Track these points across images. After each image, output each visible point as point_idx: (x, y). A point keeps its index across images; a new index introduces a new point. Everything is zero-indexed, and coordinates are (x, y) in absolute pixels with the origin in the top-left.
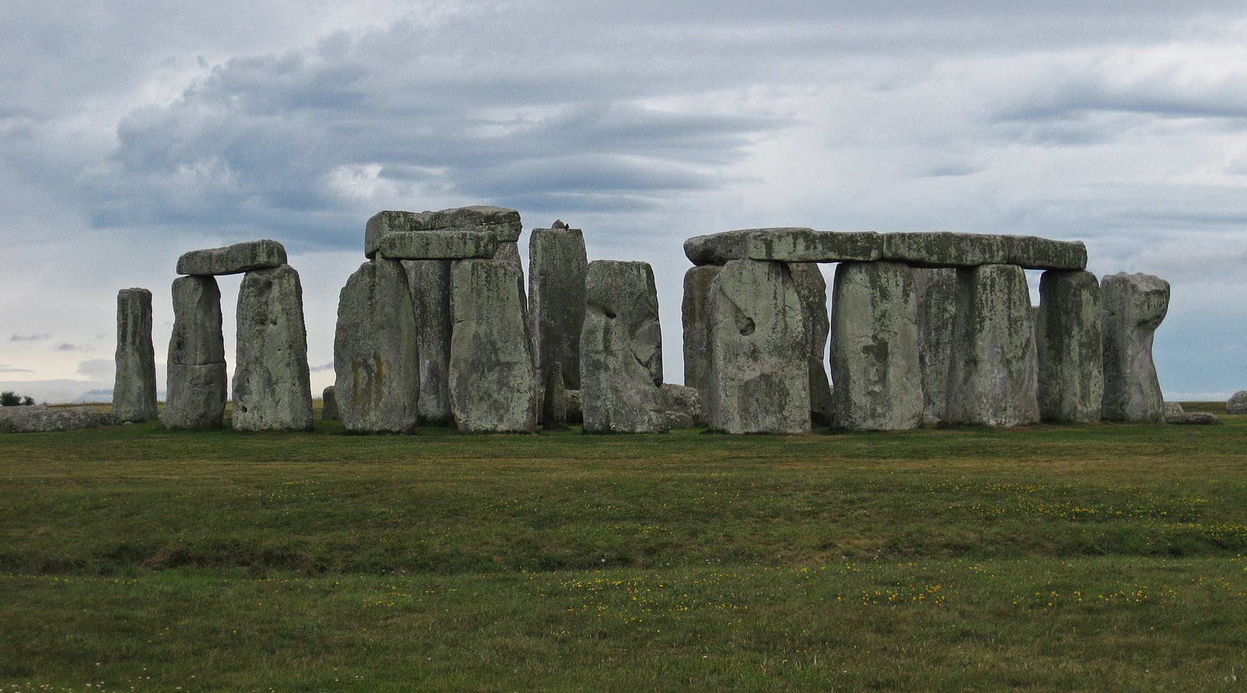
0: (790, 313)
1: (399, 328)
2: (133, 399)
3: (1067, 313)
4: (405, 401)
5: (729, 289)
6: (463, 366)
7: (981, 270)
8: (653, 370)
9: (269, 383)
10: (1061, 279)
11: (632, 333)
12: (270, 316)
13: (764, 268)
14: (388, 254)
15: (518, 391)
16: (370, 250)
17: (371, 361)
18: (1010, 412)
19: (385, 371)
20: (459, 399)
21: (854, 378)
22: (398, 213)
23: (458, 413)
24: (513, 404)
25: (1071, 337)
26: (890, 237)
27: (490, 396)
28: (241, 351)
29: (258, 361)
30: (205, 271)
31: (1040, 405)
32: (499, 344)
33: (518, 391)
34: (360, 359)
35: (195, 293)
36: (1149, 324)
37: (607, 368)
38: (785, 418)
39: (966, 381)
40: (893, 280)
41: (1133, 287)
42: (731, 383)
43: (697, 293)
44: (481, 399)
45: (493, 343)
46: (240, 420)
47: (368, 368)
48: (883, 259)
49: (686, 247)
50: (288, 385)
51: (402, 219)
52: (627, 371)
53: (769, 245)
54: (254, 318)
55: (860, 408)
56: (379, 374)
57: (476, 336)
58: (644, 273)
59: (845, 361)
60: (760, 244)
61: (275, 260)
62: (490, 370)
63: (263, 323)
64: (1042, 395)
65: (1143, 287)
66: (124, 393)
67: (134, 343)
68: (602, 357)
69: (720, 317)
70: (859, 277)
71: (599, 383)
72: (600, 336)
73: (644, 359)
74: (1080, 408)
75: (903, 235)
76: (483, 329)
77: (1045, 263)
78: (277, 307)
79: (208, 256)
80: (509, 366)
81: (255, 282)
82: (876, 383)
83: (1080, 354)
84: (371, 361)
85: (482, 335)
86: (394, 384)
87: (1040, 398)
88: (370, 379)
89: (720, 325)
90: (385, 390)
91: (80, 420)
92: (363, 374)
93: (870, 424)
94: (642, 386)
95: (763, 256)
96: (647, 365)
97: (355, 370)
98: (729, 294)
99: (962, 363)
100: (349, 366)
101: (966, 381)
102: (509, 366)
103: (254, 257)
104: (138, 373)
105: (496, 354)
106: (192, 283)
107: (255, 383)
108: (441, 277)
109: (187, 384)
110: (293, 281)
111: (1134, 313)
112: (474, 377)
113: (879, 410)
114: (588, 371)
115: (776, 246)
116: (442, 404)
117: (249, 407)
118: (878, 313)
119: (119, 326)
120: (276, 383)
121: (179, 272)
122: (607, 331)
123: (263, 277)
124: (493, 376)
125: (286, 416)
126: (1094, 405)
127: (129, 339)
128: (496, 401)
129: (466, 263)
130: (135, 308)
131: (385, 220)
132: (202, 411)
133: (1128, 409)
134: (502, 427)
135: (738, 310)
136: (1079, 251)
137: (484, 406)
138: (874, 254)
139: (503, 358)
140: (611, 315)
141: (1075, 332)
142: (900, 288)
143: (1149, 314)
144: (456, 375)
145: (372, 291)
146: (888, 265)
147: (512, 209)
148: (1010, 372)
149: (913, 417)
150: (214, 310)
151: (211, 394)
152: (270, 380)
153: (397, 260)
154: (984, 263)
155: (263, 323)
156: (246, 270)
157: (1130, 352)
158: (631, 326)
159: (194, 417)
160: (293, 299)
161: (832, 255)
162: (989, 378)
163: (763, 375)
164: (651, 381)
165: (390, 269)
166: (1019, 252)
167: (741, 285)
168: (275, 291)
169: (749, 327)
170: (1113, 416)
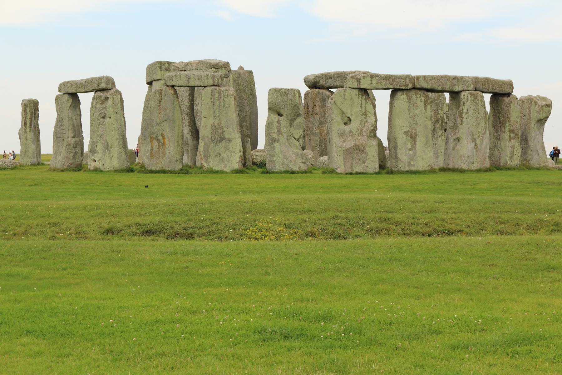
0: (369, 114)
1: (174, 121)
2: (30, 155)
3: (503, 115)
4: (177, 157)
5: (338, 103)
6: (206, 140)
7: (462, 94)
8: (301, 143)
9: (107, 147)
10: (500, 98)
11: (291, 124)
12: (108, 114)
13: (356, 92)
14: (168, 84)
15: (234, 152)
16: (149, 80)
17: (160, 137)
18: (476, 164)
19: (167, 142)
20: (204, 156)
21: (399, 147)
23: (204, 164)
24: (231, 159)
25: (505, 127)
26: (418, 78)
27: (220, 155)
28: (92, 132)
29: (101, 136)
30: (73, 91)
31: (491, 161)
32: (225, 129)
33: (234, 152)
34: (154, 136)
35: (67, 101)
36: (542, 122)
37: (278, 141)
38: (367, 167)
39: (454, 149)
40: (418, 98)
41: (535, 103)
42: (340, 149)
43: (311, 104)
44: (216, 156)
45: (223, 128)
46: (91, 165)
47: (158, 140)
48: (414, 88)
49: (305, 81)
50: (117, 149)
51: (167, 65)
52: (289, 143)
53: (358, 80)
54: (99, 116)
55: (402, 162)
56: (164, 144)
57: (213, 125)
58: (297, 94)
59: (395, 138)
60: (354, 80)
61: (110, 86)
62: (220, 141)
63: (104, 117)
64: (491, 155)
65: (541, 103)
66: (25, 152)
67: (31, 127)
68: (275, 136)
69: (334, 116)
70: (401, 97)
71: (274, 149)
72: (276, 124)
73: (297, 137)
74: (509, 163)
75: (424, 77)
76: (216, 122)
77: (493, 91)
78: (111, 109)
79: (75, 84)
80: (230, 140)
81: (100, 97)
82: (410, 150)
83: (510, 136)
84: (160, 137)
85: (216, 124)
86: (172, 149)
87: (489, 157)
88: (159, 146)
89: (335, 120)
90: (167, 152)
91: (8, 166)
92: (155, 143)
93: (407, 169)
94: (295, 150)
95: (356, 86)
96: (298, 140)
97: (151, 141)
98: (338, 105)
99: (452, 140)
100: (149, 139)
101: (454, 149)
102: (230, 140)
103: (99, 84)
104: (33, 142)
105: (223, 134)
106: (66, 97)
108: (190, 95)
109: (64, 148)
110: (119, 97)
111: (536, 116)
112: (212, 145)
113: (412, 163)
114: (269, 142)
115: (362, 81)
116: (190, 159)
118: (412, 114)
119: (23, 118)
120: (111, 147)
121: (60, 91)
122: (279, 122)
123: (103, 95)
124: (223, 144)
125: (116, 164)
126: (516, 161)
127: (28, 125)
128: (223, 157)
129: (207, 88)
130: (31, 109)
132: (71, 161)
133: (532, 163)
134: (225, 170)
135: (343, 113)
136: (510, 85)
137: (217, 159)
138: (410, 86)
139: (227, 136)
140: (280, 115)
141: (507, 125)
142: (423, 103)
143: (543, 116)
144: (203, 144)
145: (160, 102)
146: (417, 91)
147: (226, 61)
148: (476, 145)
149: (429, 166)
150: (77, 110)
151: (76, 153)
153: (173, 87)
154: (463, 91)
155: (104, 117)
156: (96, 91)
157: (533, 135)
158: (291, 120)
159: (68, 164)
160: (119, 106)
161: (389, 86)
162: (466, 148)
163: (355, 145)
164: (300, 148)
165: (169, 91)
166: (480, 85)
167: (342, 100)
168: (110, 102)
169: (348, 121)
170: (525, 166)
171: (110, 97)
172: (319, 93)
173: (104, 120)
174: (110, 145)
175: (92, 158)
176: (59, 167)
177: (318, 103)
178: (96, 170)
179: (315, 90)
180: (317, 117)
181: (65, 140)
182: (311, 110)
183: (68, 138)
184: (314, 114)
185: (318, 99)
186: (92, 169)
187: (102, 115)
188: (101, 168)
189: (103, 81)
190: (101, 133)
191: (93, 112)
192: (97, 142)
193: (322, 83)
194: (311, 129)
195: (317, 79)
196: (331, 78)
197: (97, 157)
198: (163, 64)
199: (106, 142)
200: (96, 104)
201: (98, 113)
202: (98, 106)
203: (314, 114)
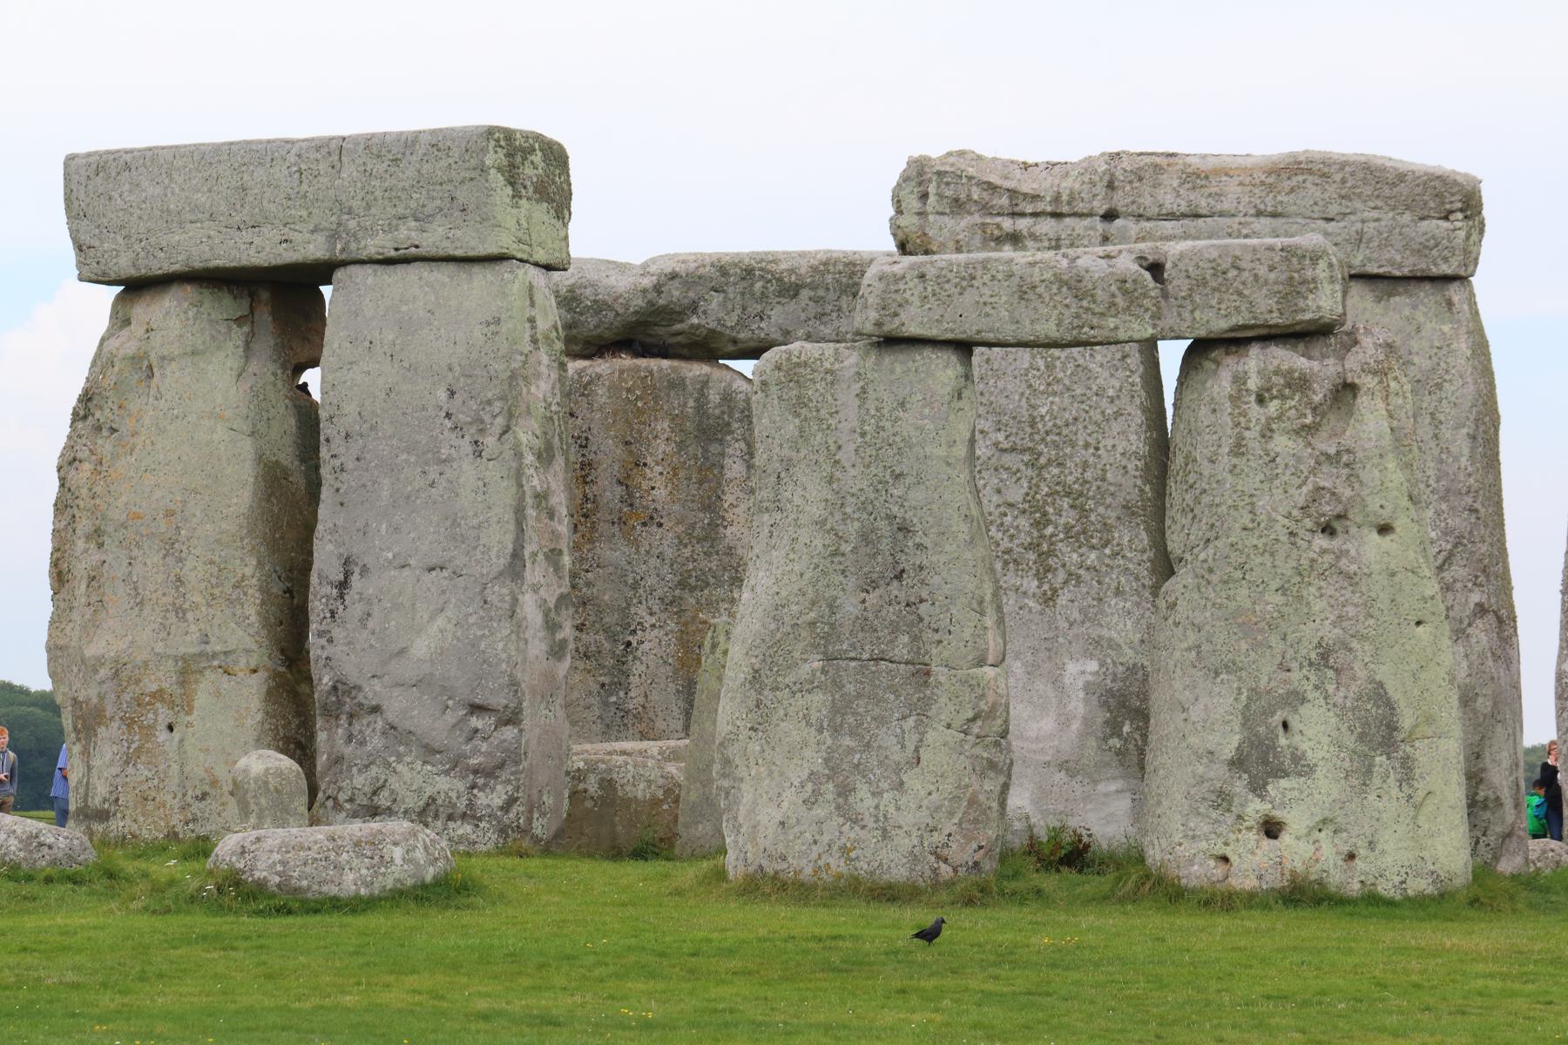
9: (1380, 733)
12: (1374, 503)
22: (527, 136)
51: (537, 158)
63: (1328, 530)
81: (1300, 383)
103: (1296, 288)
107: (1317, 731)
117: (1296, 820)
120: (1410, 739)
123: (1320, 367)
131: (494, 158)
152: (1392, 728)
168: (1371, 421)
171: (1368, 382)
172: (677, 384)
173: (1335, 544)
174: (1406, 721)
175: (1256, 808)
176: (899, 873)
177: (661, 447)
178: (1302, 895)
179: (626, 361)
180: (663, 540)
181: (940, 673)
182: (610, 494)
183: (981, 662)
184: (634, 515)
185: (663, 426)
186: (1243, 881)
187: (1328, 509)
188: (1338, 878)
189: (1321, 271)
190: (1331, 634)
191: (1252, 482)
192: (1296, 699)
193: (714, 314)
194: (611, 619)
195: (675, 293)
196: (790, 290)
197: (1297, 804)
198: (527, 152)
199: (1379, 694)
200: (1267, 433)
201: (1301, 496)
202: (1282, 443)
203: (634, 515)
